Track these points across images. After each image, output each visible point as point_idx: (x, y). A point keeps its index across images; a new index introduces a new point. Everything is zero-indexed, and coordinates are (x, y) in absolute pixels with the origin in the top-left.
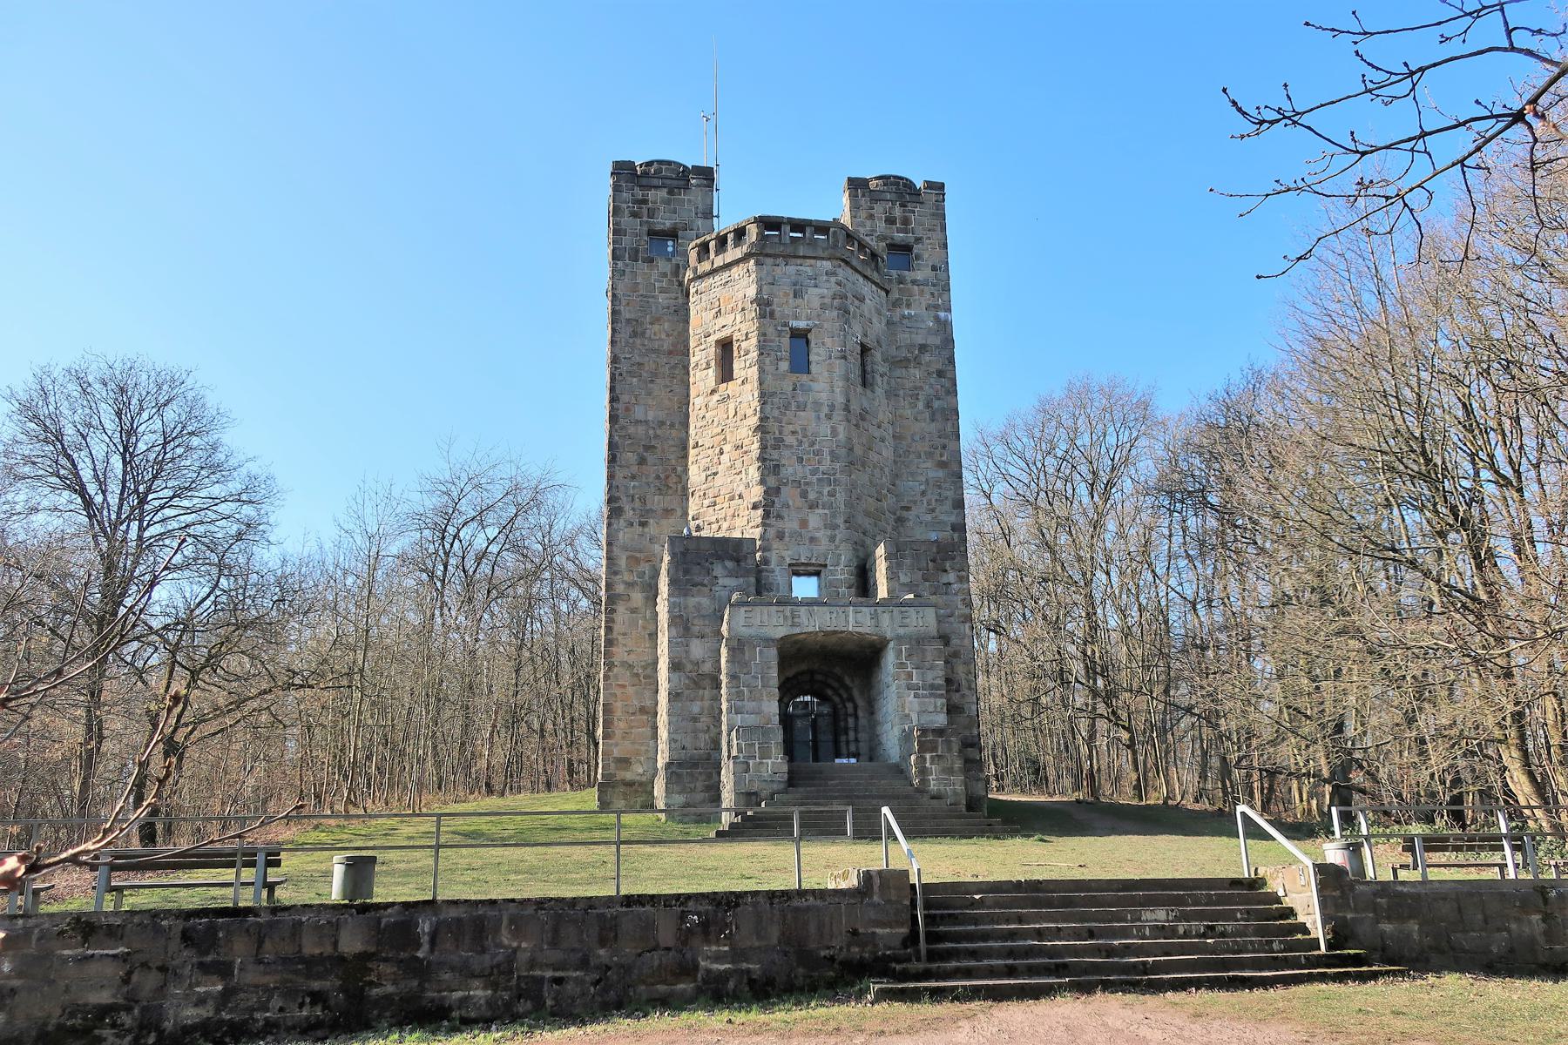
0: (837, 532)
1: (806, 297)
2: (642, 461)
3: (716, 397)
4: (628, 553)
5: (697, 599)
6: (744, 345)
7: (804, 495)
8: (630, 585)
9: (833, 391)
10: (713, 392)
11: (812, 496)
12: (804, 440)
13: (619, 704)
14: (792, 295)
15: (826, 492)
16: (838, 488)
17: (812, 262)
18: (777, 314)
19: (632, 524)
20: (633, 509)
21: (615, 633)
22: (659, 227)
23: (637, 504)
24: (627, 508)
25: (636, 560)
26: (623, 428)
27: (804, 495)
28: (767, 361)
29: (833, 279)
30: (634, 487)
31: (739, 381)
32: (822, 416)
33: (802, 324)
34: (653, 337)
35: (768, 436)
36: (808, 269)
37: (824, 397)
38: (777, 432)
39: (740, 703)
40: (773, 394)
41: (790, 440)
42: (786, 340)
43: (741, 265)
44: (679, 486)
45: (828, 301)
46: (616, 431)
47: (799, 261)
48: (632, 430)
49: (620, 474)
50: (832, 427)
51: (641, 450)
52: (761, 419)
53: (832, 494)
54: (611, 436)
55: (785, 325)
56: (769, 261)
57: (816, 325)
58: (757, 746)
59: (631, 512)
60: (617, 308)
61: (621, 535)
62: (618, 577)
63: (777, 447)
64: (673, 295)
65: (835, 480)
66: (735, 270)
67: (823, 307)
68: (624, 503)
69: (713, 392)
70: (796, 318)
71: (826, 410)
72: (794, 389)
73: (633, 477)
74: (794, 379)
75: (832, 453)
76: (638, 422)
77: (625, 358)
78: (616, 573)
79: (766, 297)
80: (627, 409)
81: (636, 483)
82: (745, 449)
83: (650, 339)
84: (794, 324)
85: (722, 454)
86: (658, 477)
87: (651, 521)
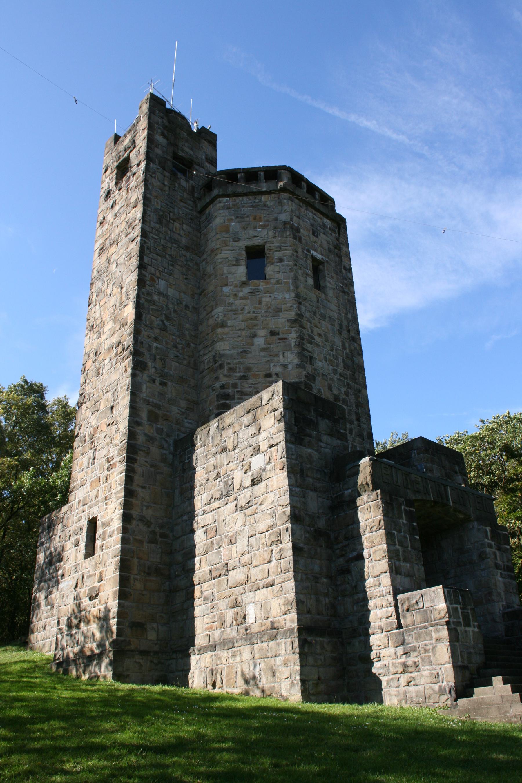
0: (353, 426)
1: (320, 238)
2: (164, 329)
3: (246, 290)
4: (150, 408)
5: (309, 451)
6: (277, 255)
7: (330, 388)
8: (150, 439)
9: (340, 314)
10: (244, 284)
11: (335, 391)
12: (327, 343)
13: (136, 561)
14: (311, 233)
15: (343, 390)
16: (349, 390)
17: (322, 217)
18: (303, 241)
19: (154, 381)
20: (155, 367)
21: (135, 484)
22: (180, 153)
23: (159, 365)
24: (150, 364)
25: (153, 418)
26: (148, 294)
27: (330, 388)
28: (300, 272)
29: (334, 235)
30: (157, 348)
31: (273, 281)
32: (336, 330)
33: (319, 257)
34: (174, 230)
35: (304, 331)
36: (319, 220)
37: (335, 315)
38: (310, 330)
39: (397, 563)
40: (305, 299)
41: (318, 339)
42: (310, 262)
43: (273, 195)
44: (192, 360)
45: (331, 247)
46: (143, 294)
47: (314, 211)
48: (156, 298)
49: (144, 333)
50: (342, 341)
51: (163, 317)
52: (297, 315)
53: (347, 394)
54: (138, 296)
55: (309, 251)
56: (296, 201)
57: (327, 261)
58: (460, 611)
59: (153, 370)
60: (148, 196)
61: (144, 387)
62: (140, 428)
63: (310, 343)
64: (190, 208)
65: (348, 384)
66: (263, 198)
67: (330, 250)
68: (147, 358)
69: (244, 284)
70: (316, 251)
71: (337, 327)
72: (318, 302)
73: (156, 339)
74: (317, 293)
75: (344, 361)
76: (160, 294)
77: (153, 237)
78: (138, 424)
79: (296, 225)
80: (152, 280)
81: (159, 346)
82: (281, 336)
83: (172, 231)
84: (315, 254)
85: (255, 336)
86: (176, 347)
87: (169, 383)
